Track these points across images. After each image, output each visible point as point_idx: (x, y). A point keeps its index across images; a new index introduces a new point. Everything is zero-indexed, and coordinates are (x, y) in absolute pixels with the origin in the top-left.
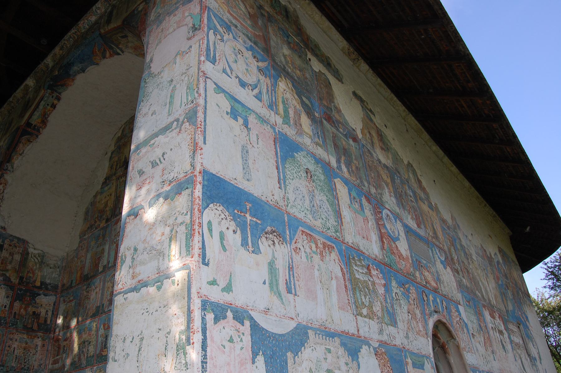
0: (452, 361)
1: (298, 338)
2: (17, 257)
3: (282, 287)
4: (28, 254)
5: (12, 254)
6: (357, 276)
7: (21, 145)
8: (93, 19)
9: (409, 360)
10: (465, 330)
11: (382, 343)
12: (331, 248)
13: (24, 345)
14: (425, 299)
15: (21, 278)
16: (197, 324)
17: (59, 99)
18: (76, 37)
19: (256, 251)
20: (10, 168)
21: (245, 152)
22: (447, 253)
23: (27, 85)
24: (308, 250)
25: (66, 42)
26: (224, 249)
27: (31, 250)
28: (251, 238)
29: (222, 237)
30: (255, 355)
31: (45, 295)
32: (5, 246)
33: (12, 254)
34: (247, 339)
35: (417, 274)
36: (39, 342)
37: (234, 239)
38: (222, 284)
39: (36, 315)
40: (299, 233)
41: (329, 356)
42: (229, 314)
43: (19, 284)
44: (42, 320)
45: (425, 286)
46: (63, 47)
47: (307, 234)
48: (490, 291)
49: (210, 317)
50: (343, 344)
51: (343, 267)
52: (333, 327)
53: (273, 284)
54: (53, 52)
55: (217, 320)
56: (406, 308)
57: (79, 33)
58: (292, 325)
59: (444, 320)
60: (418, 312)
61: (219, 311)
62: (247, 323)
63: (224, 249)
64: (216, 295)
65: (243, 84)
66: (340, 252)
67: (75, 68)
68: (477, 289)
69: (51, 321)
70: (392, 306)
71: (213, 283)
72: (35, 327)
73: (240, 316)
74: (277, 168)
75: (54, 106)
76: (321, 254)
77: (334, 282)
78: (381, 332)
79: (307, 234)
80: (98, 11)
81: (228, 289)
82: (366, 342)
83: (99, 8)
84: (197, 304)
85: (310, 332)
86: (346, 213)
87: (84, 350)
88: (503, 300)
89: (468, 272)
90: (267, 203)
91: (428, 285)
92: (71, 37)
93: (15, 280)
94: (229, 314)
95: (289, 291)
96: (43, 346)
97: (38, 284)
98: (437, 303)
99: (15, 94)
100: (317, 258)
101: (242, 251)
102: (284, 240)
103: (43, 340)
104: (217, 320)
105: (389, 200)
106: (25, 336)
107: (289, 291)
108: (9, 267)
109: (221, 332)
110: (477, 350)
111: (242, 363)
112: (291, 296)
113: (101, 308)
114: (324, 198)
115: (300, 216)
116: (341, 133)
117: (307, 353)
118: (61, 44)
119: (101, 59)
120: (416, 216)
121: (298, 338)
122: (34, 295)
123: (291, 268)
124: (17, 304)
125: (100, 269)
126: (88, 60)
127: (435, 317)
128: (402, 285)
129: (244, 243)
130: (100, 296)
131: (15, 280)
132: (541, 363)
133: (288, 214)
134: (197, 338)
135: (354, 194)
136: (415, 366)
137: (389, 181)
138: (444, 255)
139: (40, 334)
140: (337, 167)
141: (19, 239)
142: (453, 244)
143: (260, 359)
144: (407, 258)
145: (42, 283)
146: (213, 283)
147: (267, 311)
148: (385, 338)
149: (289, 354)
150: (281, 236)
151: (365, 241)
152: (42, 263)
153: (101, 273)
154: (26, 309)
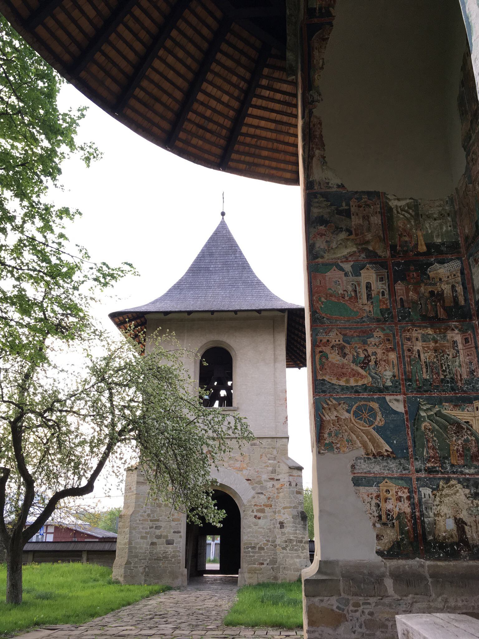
2: (376, 220)
4: (391, 209)
5: (366, 218)
7: (316, 53)
13: (432, 345)
15: (393, 248)
20: (316, 97)
27: (393, 203)
31: (442, 262)
32: (353, 210)
33: (366, 218)
36: (458, 338)
39: (438, 296)
43: (392, 256)
44: (449, 303)
69: (466, 300)
72: (442, 314)
93: (384, 253)
96: (466, 340)
97: (423, 248)
103: (462, 331)
106: (430, 331)
108: (369, 237)
122: (423, 268)
124: (399, 287)
131: (384, 253)
139: (453, 324)
141: (369, 194)
145: (429, 246)
152: (417, 216)
154: (416, 291)
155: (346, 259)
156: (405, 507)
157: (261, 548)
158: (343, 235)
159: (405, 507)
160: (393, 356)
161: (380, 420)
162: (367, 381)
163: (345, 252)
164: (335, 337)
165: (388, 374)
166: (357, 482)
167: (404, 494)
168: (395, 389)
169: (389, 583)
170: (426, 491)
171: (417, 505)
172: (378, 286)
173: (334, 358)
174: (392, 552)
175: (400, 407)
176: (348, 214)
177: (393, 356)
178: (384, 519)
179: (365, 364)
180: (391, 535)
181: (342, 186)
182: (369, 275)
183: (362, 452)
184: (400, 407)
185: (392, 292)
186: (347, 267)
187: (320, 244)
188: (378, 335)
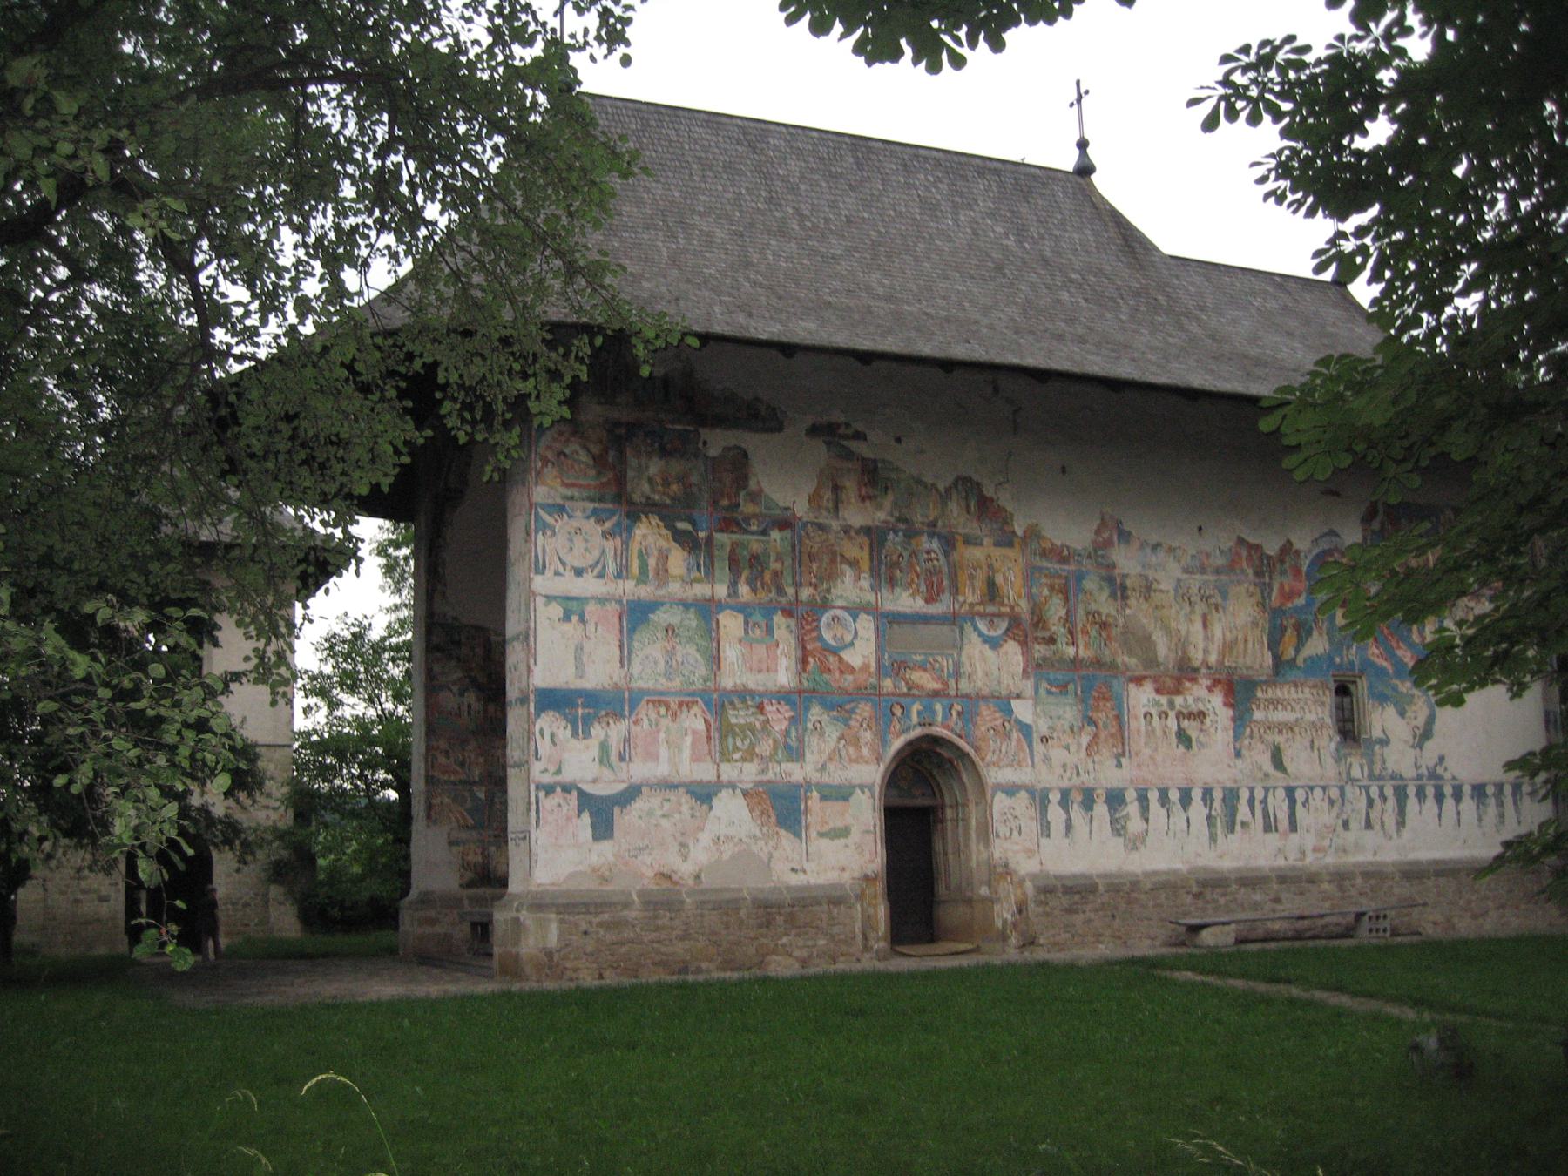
0: (965, 779)
1: (631, 794)
3: (614, 757)
5: (472, 649)
6: (733, 721)
9: (815, 794)
10: (1015, 735)
11: (759, 783)
12: (689, 705)
14: (898, 711)
16: (533, 799)
19: (587, 735)
21: (579, 649)
22: (1026, 617)
24: (653, 716)
26: (554, 744)
28: (581, 729)
29: (552, 736)
30: (580, 812)
33: (472, 649)
34: (574, 803)
35: (888, 684)
37: (564, 733)
38: (552, 769)
40: (644, 702)
41: (667, 805)
42: (558, 789)
45: (905, 695)
47: (653, 702)
48: (1208, 638)
49: (542, 794)
50: (691, 792)
51: (709, 717)
52: (676, 780)
53: (604, 759)
55: (547, 794)
56: (835, 735)
58: (624, 786)
59: (945, 733)
60: (867, 736)
61: (549, 790)
62: (575, 793)
63: (554, 744)
64: (547, 779)
65: (579, 572)
66: (707, 704)
68: (1131, 653)
70: (800, 740)
71: (546, 770)
73: (567, 789)
74: (621, 647)
75: (469, 465)
76: (674, 715)
77: (689, 739)
78: (763, 771)
79: (653, 702)
81: (559, 771)
82: (732, 786)
84: (533, 787)
85: (645, 790)
86: (731, 653)
88: (1274, 644)
89: (1104, 626)
90: (604, 690)
91: (915, 692)
94: (558, 789)
95: (622, 758)
98: (934, 712)
100: (665, 722)
101: (574, 742)
102: (623, 716)
104: (547, 794)
105: (851, 587)
107: (622, 758)
109: (548, 803)
110: (1047, 759)
111: (569, 819)
112: (624, 765)
114: (691, 650)
115: (645, 686)
116: (752, 533)
117: (638, 806)
120: (930, 585)
121: (631, 794)
123: (627, 740)
127: (917, 732)
128: (828, 707)
129: (575, 734)
132: (1420, 746)
133: (630, 690)
134: (533, 807)
135: (757, 617)
136: (823, 798)
137: (866, 554)
138: (1004, 625)
140: (729, 595)
142: (1067, 590)
143: (586, 817)
144: (865, 667)
146: (546, 770)
147: (595, 781)
148: (770, 776)
149: (616, 810)
150: (618, 715)
151: (762, 677)
155: (454, 683)
156: (479, 859)
157: (246, 905)
158: (453, 663)
159: (479, 859)
160: (481, 760)
161: (469, 804)
162: (463, 777)
163: (455, 676)
164: (443, 744)
165: (477, 773)
166: (451, 844)
167: (479, 851)
168: (480, 783)
169: (466, 902)
170: (493, 849)
171: (486, 856)
172: (477, 706)
173: (442, 760)
174: (470, 884)
175: (482, 795)
176: (458, 643)
177: (481, 760)
178: (465, 866)
179: (462, 764)
180: (469, 875)
181: (455, 619)
182: (471, 698)
183: (455, 824)
184: (482, 795)
185: (485, 711)
186: (455, 689)
187: (437, 668)
188: (472, 745)
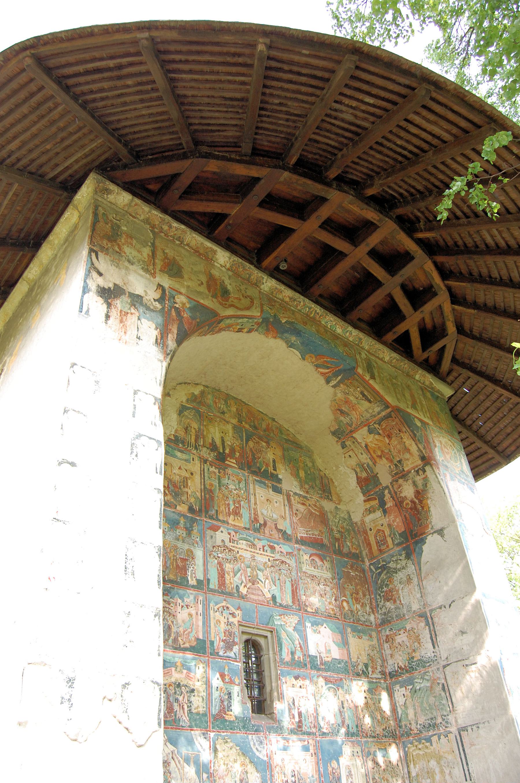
8: (339, 331)
17: (250, 331)
18: (312, 315)
23: (215, 252)
25: (302, 303)
46: (295, 300)
54: (282, 287)
57: (318, 317)
67: (293, 339)
80: (348, 334)
83: (351, 334)
87: (181, 698)
92: (310, 308)
99: (188, 230)
113: (208, 644)
118: (297, 295)
119: (313, 363)
125: (192, 582)
126: (307, 350)
130: (200, 623)
153: (193, 586)
